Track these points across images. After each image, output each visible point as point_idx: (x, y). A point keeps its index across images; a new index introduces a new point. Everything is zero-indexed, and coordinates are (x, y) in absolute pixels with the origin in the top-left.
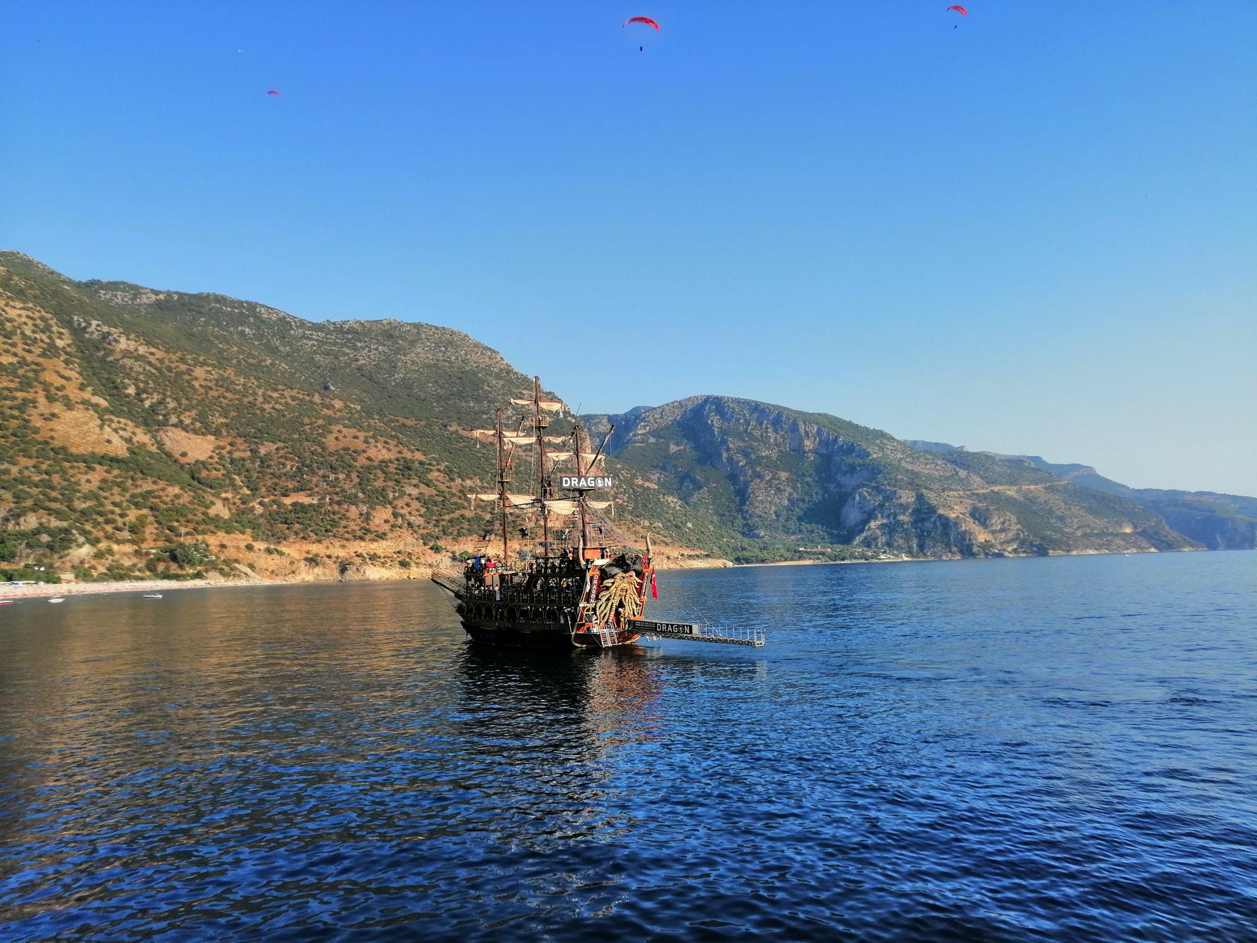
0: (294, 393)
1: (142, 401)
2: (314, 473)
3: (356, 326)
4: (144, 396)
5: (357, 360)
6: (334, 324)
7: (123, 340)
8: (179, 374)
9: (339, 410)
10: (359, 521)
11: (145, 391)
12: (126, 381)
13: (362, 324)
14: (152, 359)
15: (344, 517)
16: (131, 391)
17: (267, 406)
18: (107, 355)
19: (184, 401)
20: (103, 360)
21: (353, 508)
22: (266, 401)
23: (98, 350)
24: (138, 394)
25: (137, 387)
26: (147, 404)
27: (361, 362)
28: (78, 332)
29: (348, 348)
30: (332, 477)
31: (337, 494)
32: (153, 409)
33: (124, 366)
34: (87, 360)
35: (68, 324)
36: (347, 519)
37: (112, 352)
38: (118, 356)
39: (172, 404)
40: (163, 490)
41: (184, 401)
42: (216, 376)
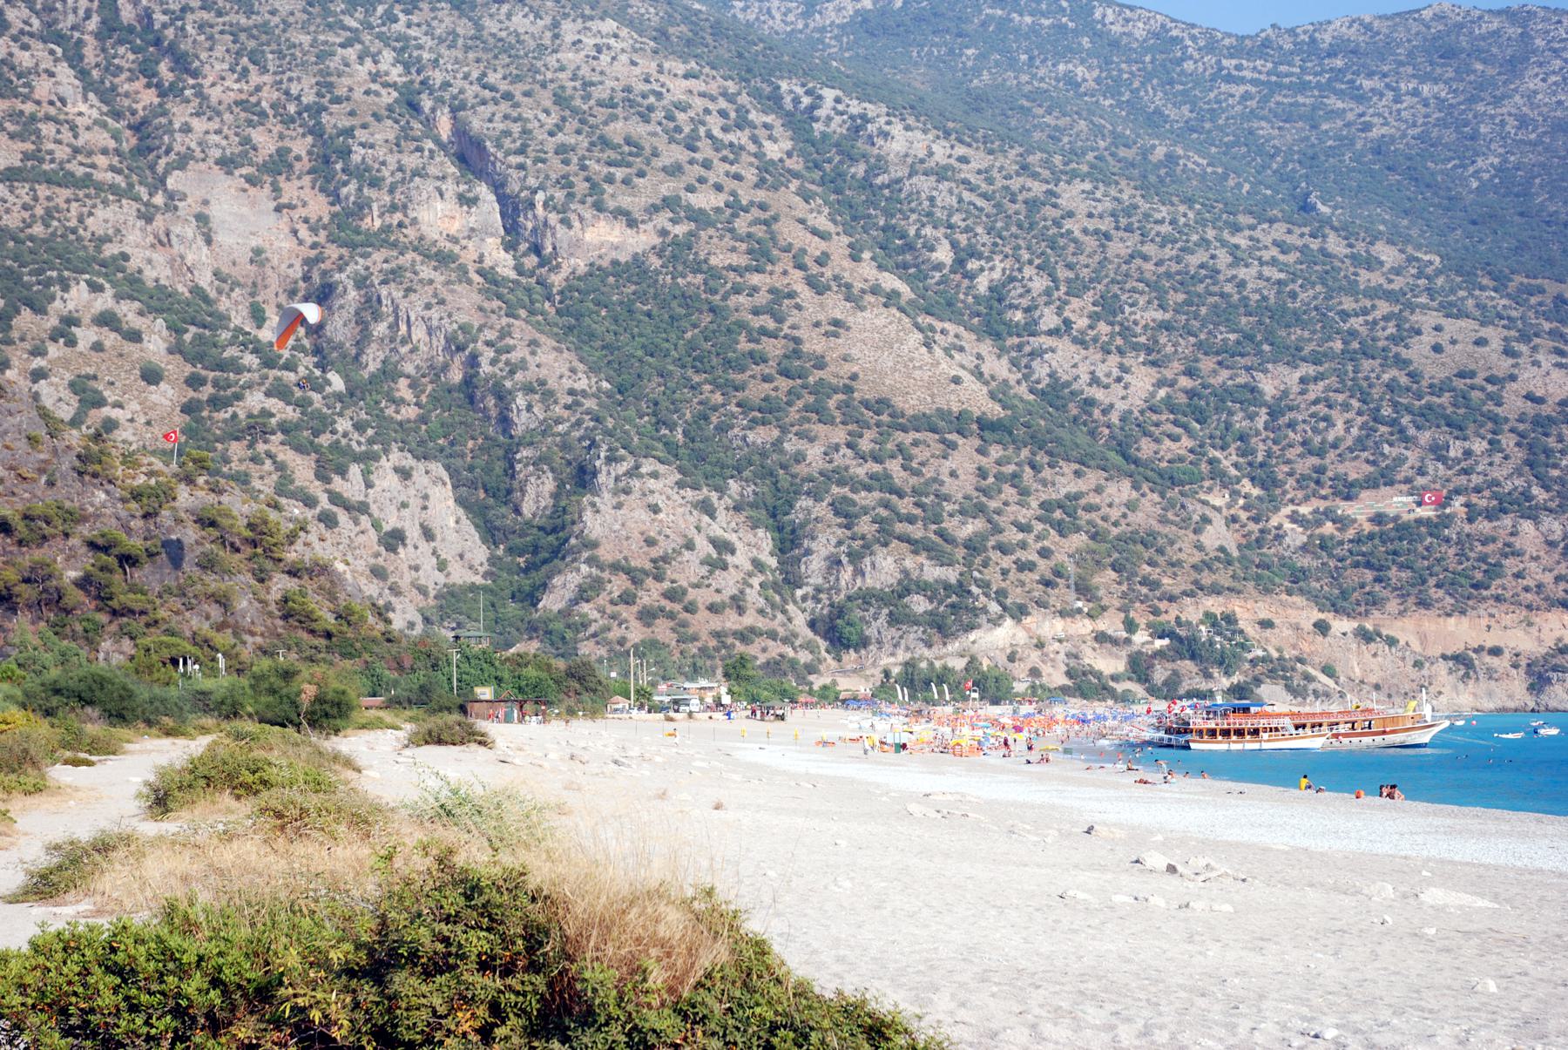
0: (1278, 232)
1: (971, 276)
2: (1407, 440)
3: (1352, 33)
4: (972, 265)
5: (1367, 127)
6: (1292, 32)
7: (897, 129)
8: (1033, 205)
9: (1397, 271)
10: (1546, 560)
11: (974, 254)
12: (928, 231)
13: (1368, 27)
14: (967, 172)
15: (1511, 551)
16: (944, 254)
17: (1242, 273)
18: (873, 171)
19: (1063, 273)
20: (866, 184)
21: (1527, 526)
22: (1237, 261)
23: (853, 160)
24: (960, 263)
25: (954, 245)
26: (982, 284)
27: (1375, 133)
28: (799, 122)
29: (1340, 94)
30: (1455, 451)
31: (1478, 490)
32: (998, 293)
33: (915, 195)
34: (834, 182)
35: (773, 101)
36: (1518, 554)
37: (879, 165)
38: (900, 172)
39: (1039, 284)
40: (1098, 490)
41: (1063, 273)
42: (1108, 205)
